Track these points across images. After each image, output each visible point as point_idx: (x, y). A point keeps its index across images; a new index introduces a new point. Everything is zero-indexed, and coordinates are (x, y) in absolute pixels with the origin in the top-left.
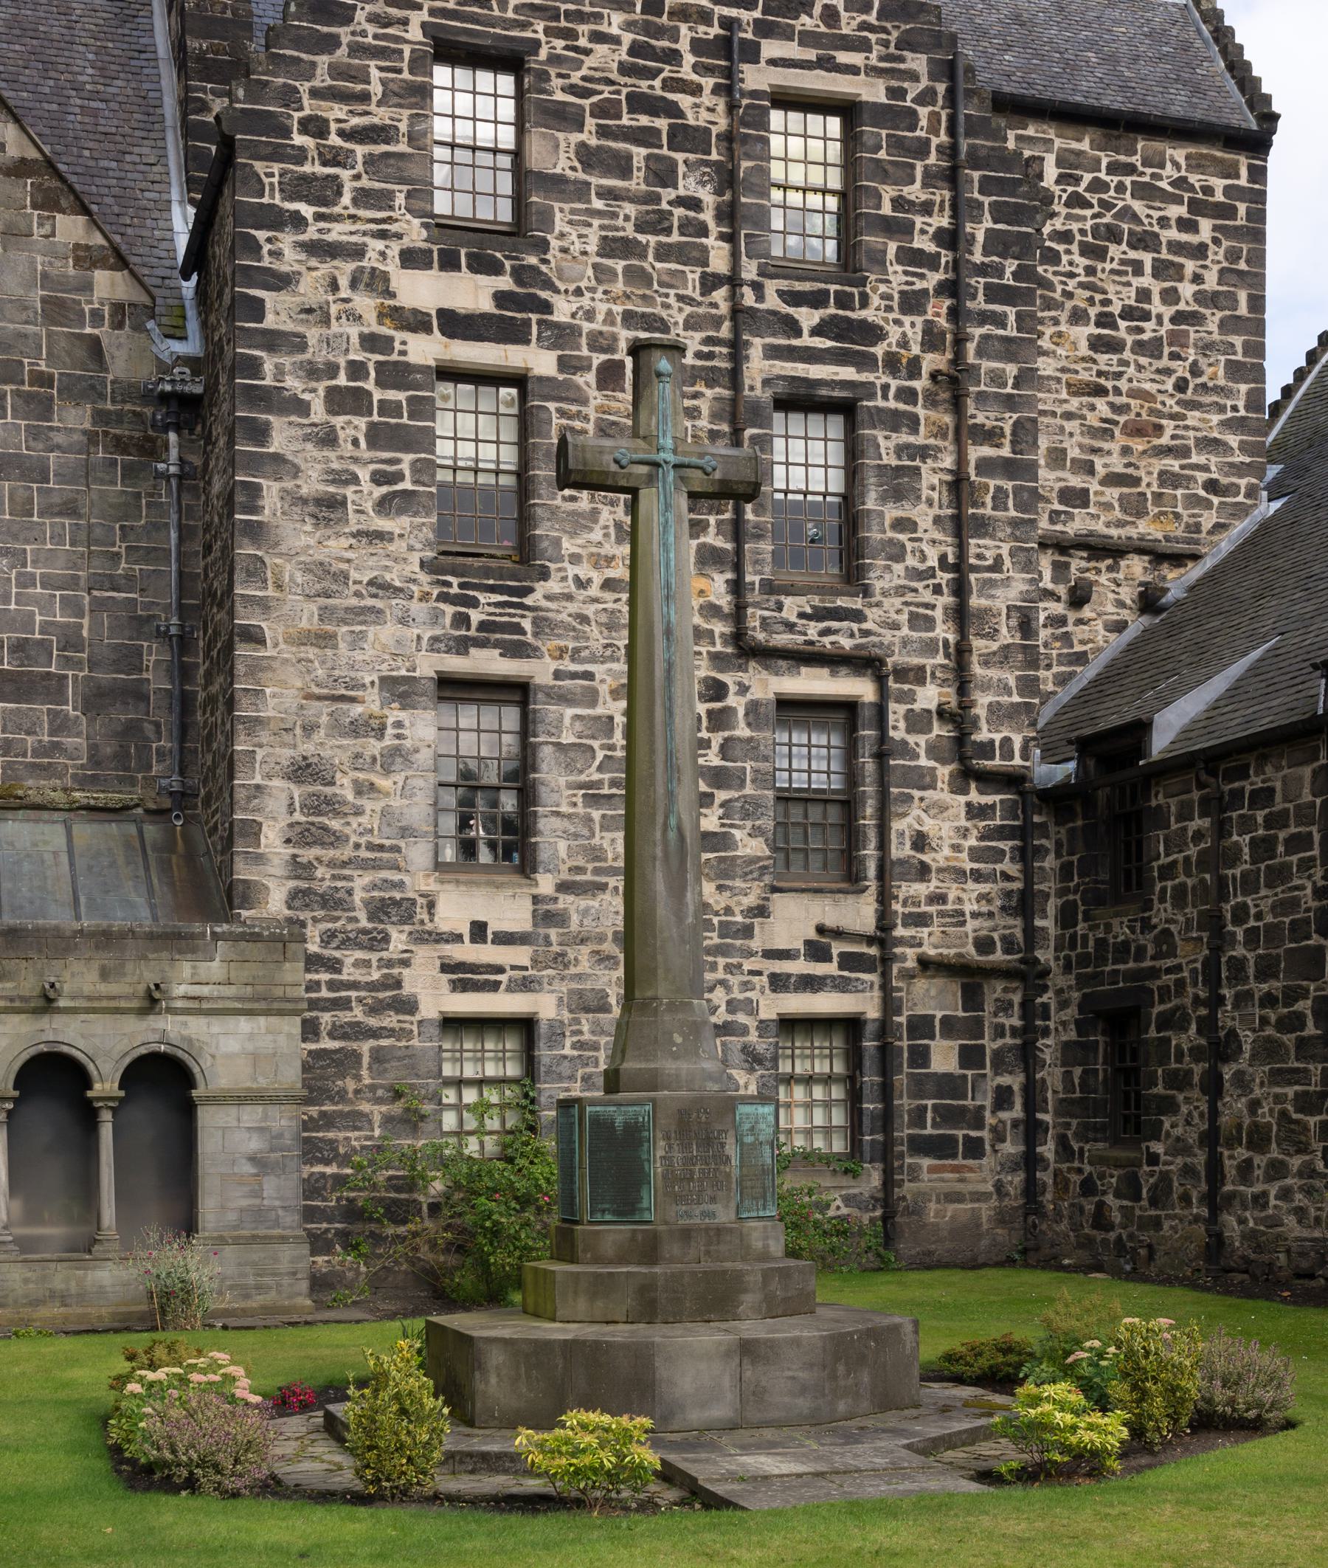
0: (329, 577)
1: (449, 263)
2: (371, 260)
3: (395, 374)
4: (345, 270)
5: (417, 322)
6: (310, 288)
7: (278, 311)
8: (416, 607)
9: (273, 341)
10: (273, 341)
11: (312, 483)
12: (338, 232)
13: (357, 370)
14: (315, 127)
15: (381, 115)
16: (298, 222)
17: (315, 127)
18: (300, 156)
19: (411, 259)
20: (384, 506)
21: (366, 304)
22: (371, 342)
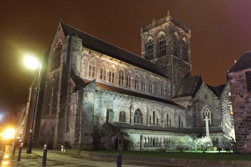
0: (225, 116)
1: (230, 101)
2: (226, 102)
3: (228, 107)
4: (225, 103)
5: (228, 104)
6: (224, 104)
7: (222, 105)
8: (230, 117)
9: (222, 106)
10: (222, 106)
11: (224, 112)
12: (225, 101)
13: (226, 107)
14: (223, 97)
15: (226, 96)
16: (223, 101)
17: (223, 97)
18: (223, 98)
19: (228, 102)
20: (228, 113)
21: (226, 104)
22: (227, 106)
